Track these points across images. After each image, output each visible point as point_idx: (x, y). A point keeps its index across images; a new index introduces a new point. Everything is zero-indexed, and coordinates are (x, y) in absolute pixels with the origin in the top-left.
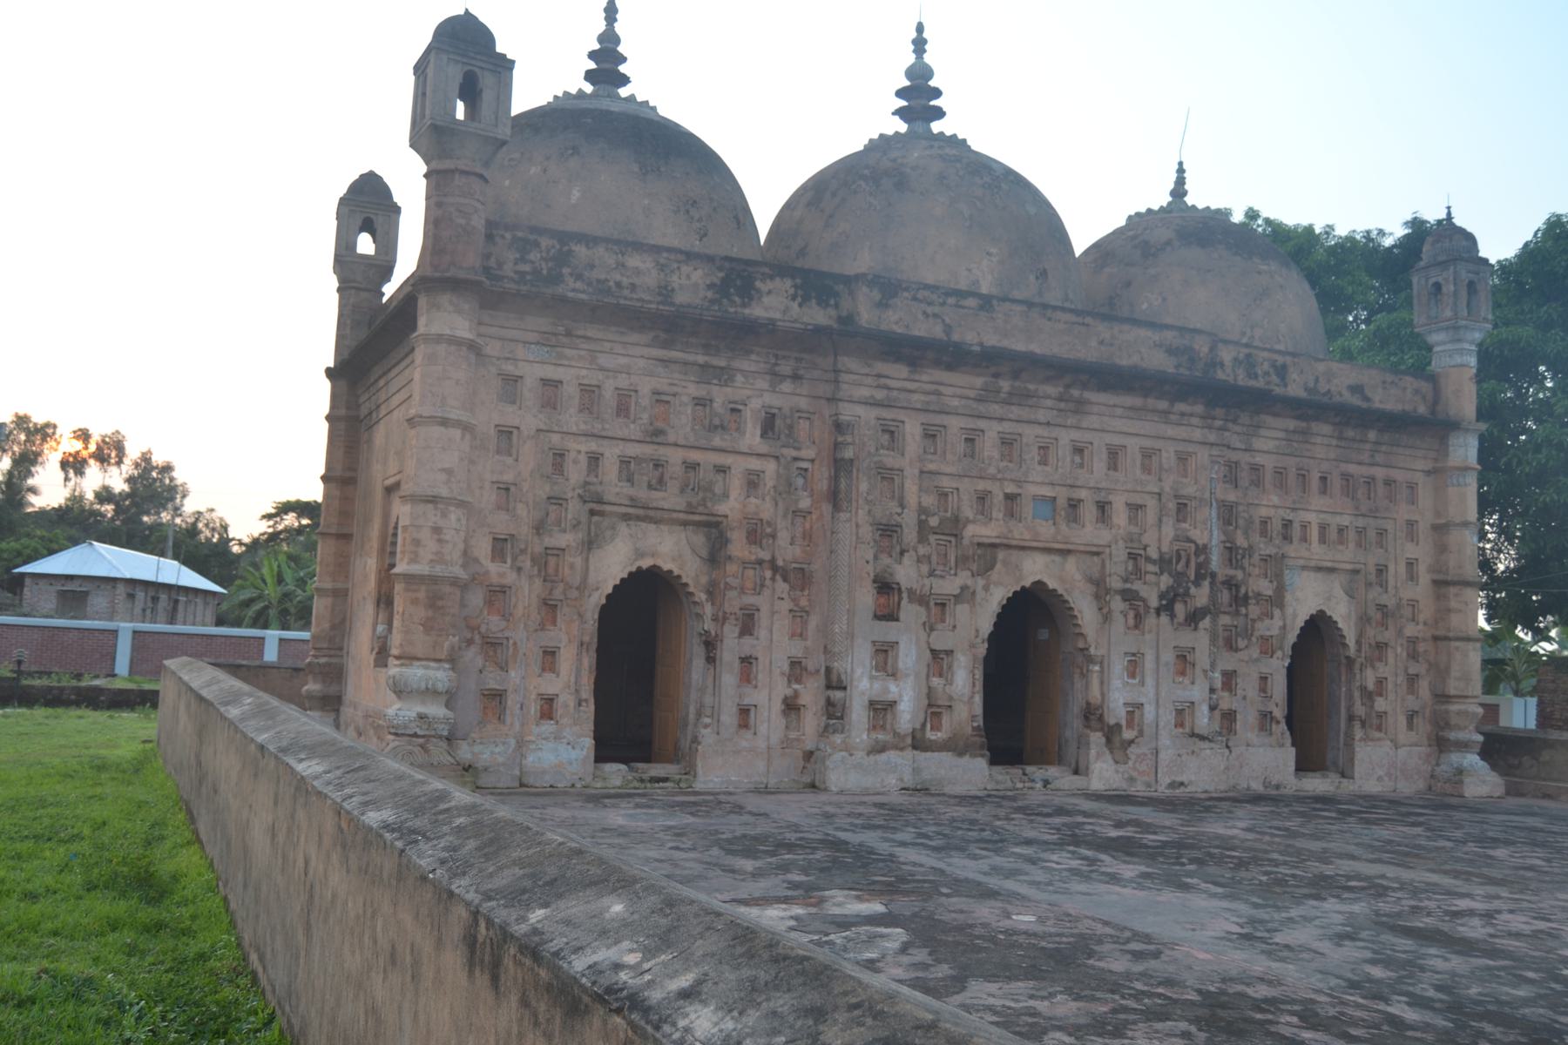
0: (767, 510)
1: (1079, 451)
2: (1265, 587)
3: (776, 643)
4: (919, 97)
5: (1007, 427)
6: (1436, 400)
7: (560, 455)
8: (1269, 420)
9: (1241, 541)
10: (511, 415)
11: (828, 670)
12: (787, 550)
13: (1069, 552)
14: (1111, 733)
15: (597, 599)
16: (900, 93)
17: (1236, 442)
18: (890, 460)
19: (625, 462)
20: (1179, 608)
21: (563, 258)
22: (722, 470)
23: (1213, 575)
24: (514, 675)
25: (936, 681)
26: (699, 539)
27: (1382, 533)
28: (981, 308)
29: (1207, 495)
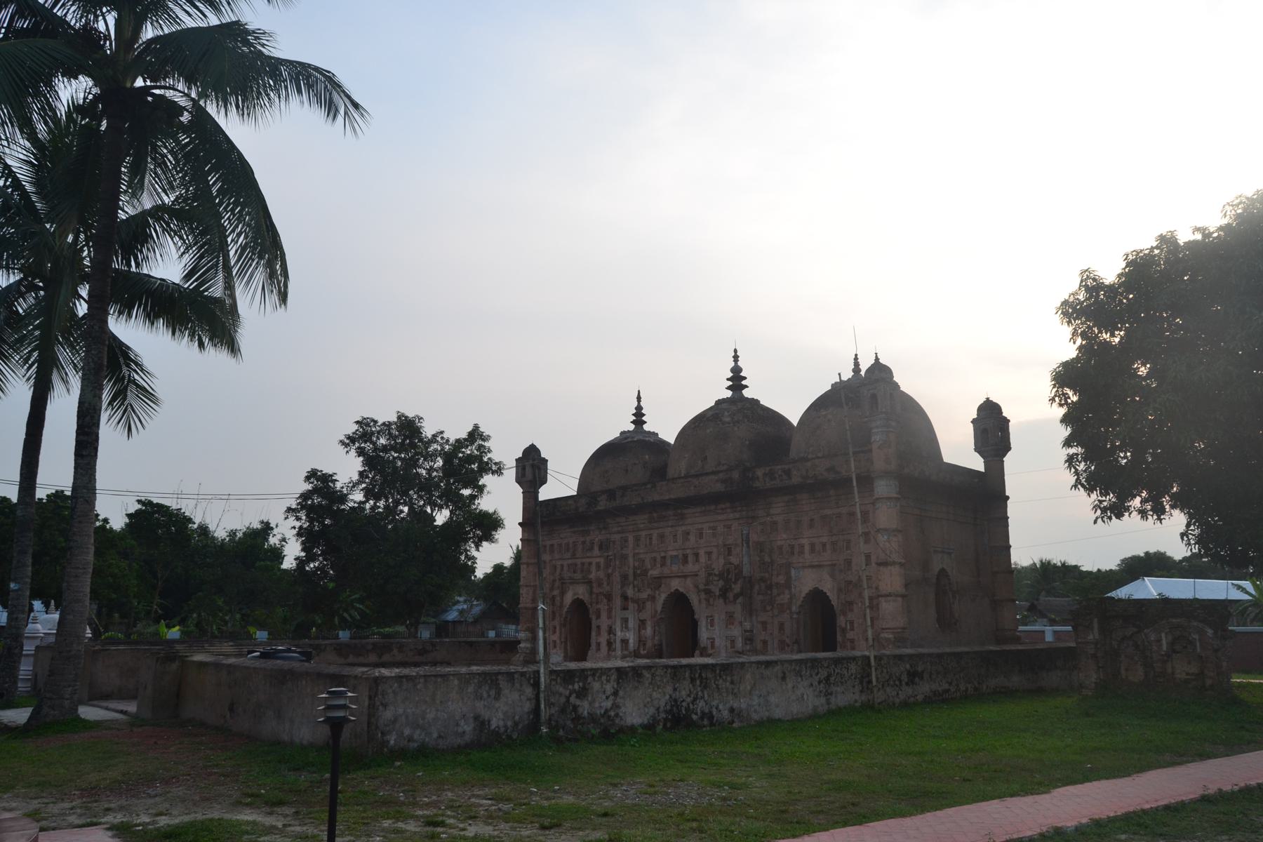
2: (781, 579)
4: (737, 381)
5: (660, 531)
7: (555, 567)
9: (767, 559)
20: (730, 595)
22: (590, 564)
27: (849, 542)
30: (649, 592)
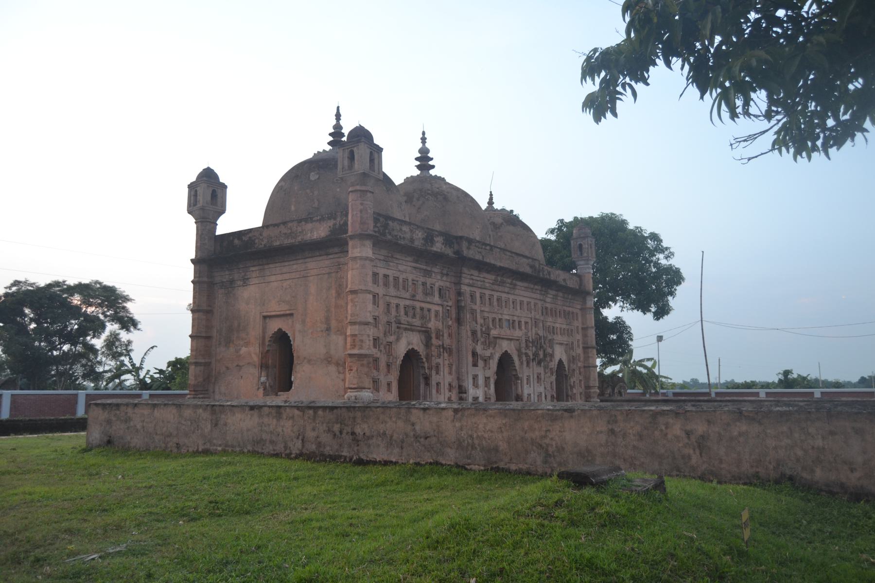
0: (440, 325)
3: (445, 377)
4: (424, 160)
5: (499, 294)
6: (581, 285)
11: (460, 387)
12: (447, 341)
15: (399, 362)
16: (417, 159)
18: (474, 307)
21: (386, 226)
22: (429, 310)
26: (423, 337)
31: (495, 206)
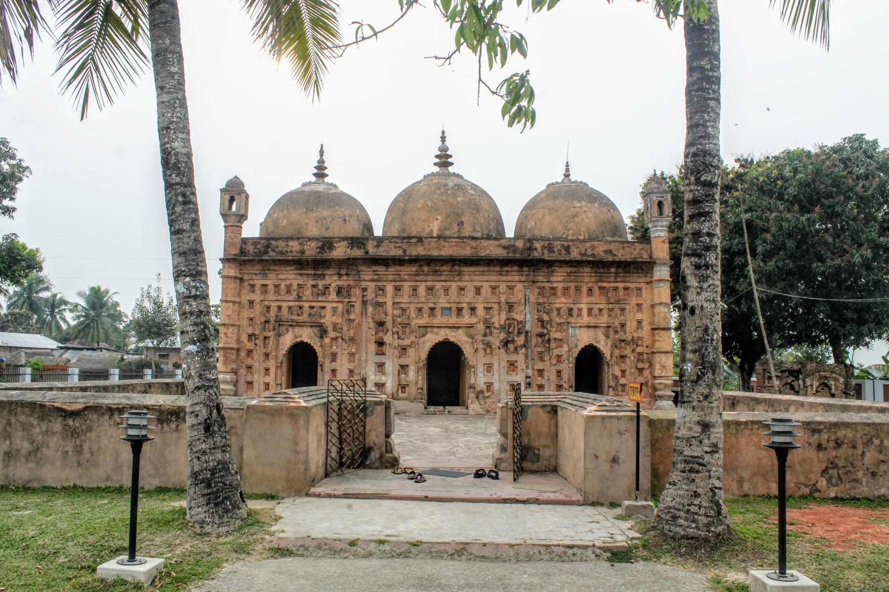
1: (462, 289)
4: (444, 160)
5: (429, 284)
7: (268, 308)
8: (557, 269)
9: (546, 318)
10: (252, 297)
13: (459, 327)
14: (479, 395)
16: (437, 156)
17: (540, 278)
18: (381, 299)
19: (290, 308)
20: (511, 346)
22: (323, 308)
23: (527, 332)
24: (256, 376)
25: (402, 376)
26: (316, 330)
27: (623, 310)
28: (418, 242)
29: (523, 301)
30: (412, 338)
31: (573, 178)
